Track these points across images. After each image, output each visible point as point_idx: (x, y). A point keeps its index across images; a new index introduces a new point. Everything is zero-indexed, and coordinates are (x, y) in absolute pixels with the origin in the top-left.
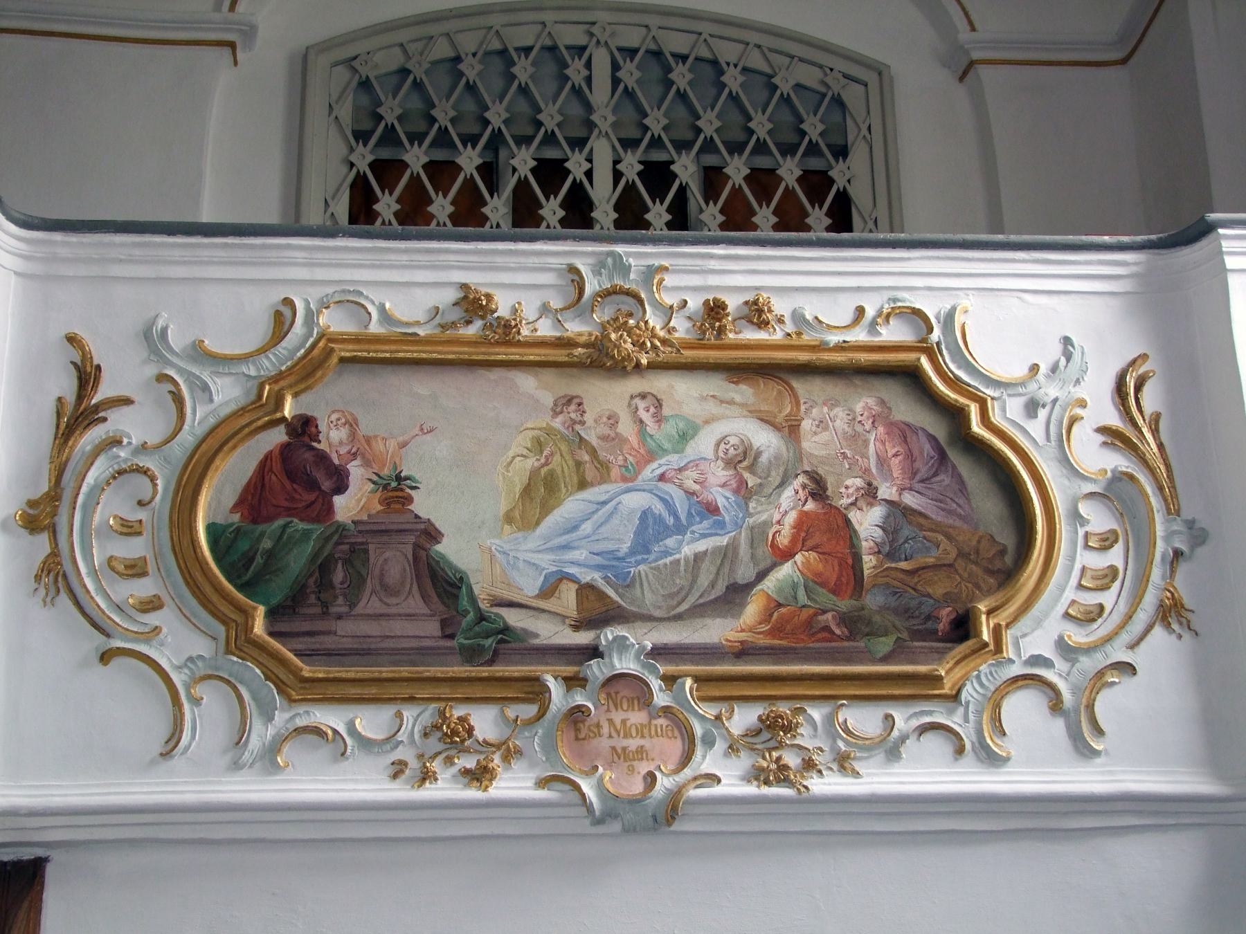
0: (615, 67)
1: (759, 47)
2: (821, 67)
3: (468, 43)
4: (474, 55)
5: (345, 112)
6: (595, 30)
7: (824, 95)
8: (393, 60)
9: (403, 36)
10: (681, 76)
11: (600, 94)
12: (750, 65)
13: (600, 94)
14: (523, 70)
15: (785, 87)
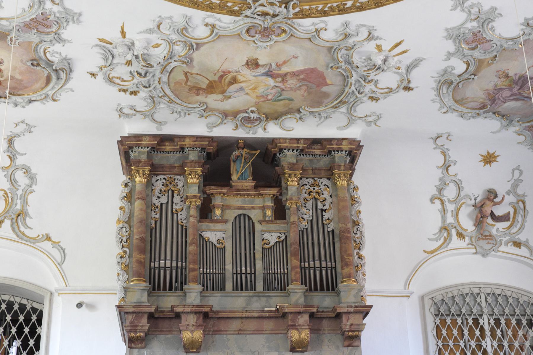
0: (486, 298)
1: (515, 292)
2: (528, 296)
3: (455, 293)
4: (457, 295)
5: (432, 310)
6: (481, 289)
7: (529, 303)
8: (441, 298)
9: (442, 292)
10: (500, 300)
11: (483, 304)
12: (514, 296)
13: (483, 304)
14: (468, 299)
15: (521, 302)
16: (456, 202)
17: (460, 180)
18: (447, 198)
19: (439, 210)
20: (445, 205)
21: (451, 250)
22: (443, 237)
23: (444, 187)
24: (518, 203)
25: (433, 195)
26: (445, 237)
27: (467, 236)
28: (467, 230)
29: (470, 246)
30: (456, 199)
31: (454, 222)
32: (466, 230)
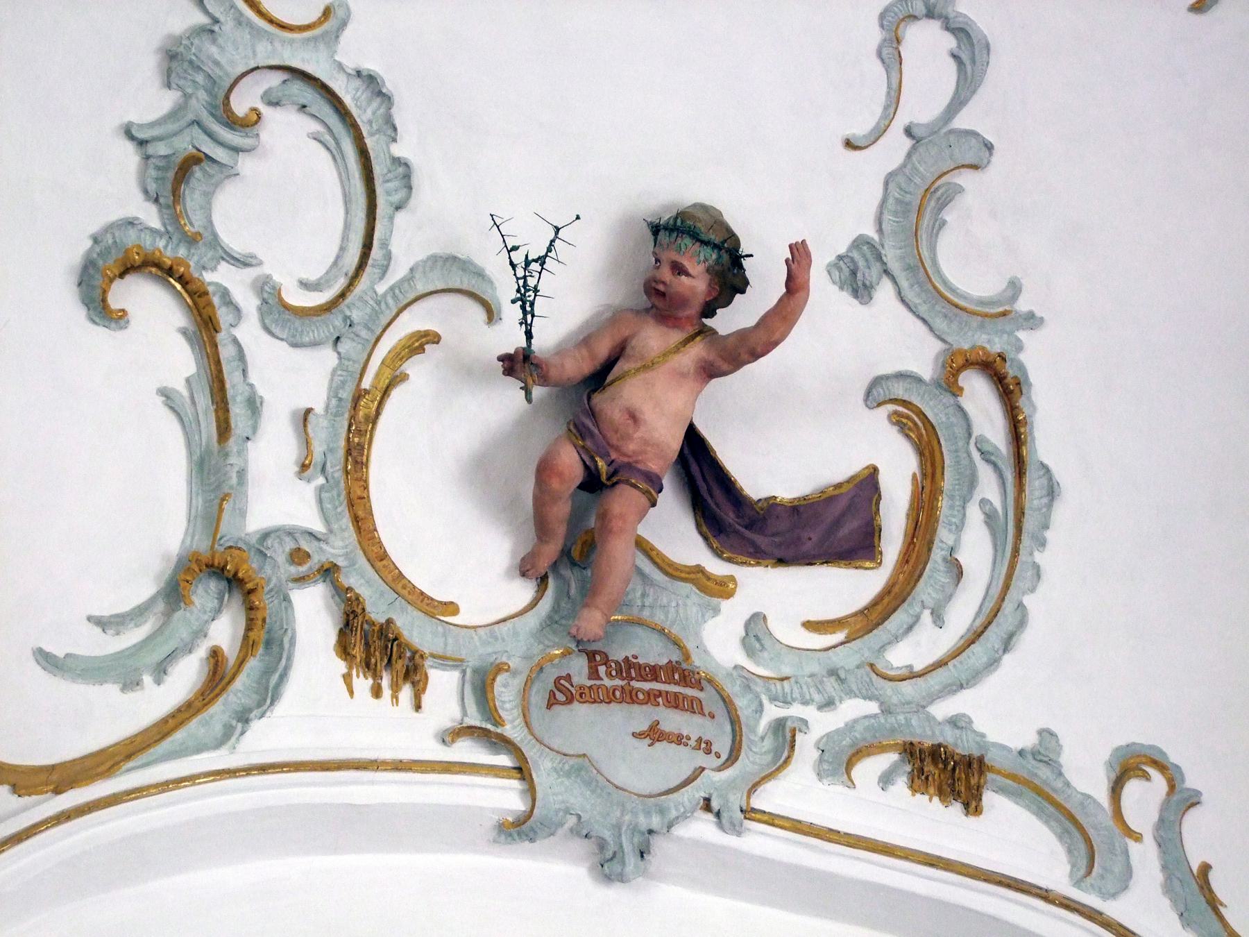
16: (336, 320)
17: (370, 81)
18: (250, 274)
19: (167, 395)
20: (226, 352)
21: (263, 769)
22: (202, 652)
23: (219, 154)
24: (949, 383)
25: (110, 228)
26: (215, 653)
27: (445, 661)
28: (451, 608)
29: (467, 751)
30: (342, 295)
31: (318, 526)
32: (439, 609)
